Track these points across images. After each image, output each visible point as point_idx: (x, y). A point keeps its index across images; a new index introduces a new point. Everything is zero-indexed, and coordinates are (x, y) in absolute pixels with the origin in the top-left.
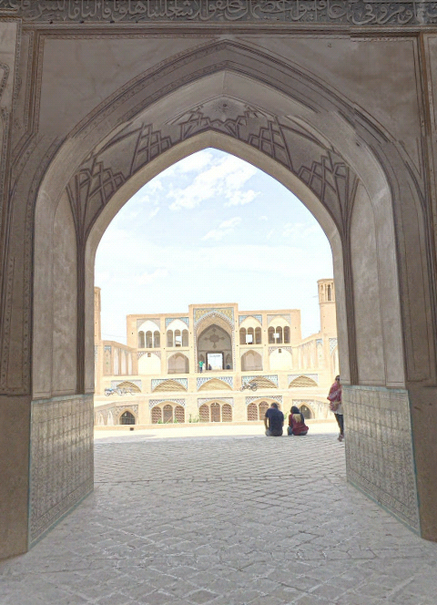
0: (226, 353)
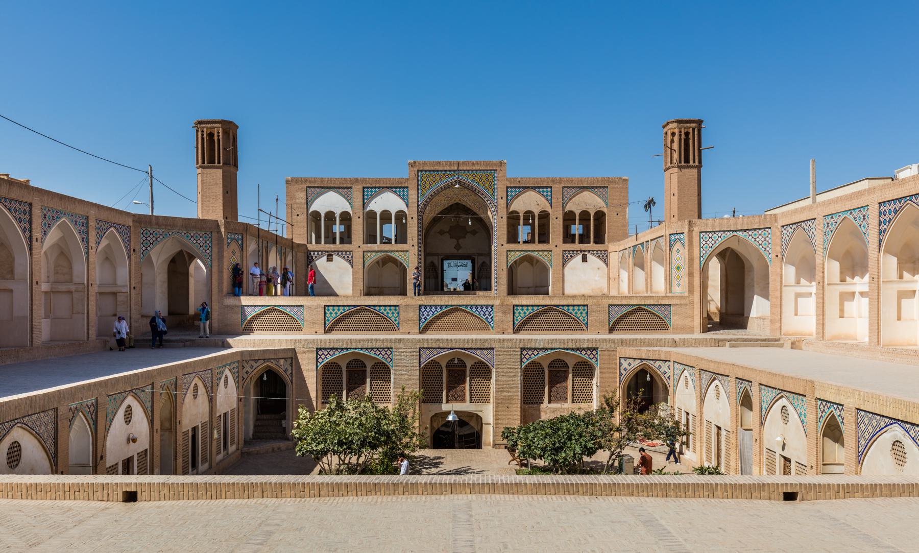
0: (479, 260)
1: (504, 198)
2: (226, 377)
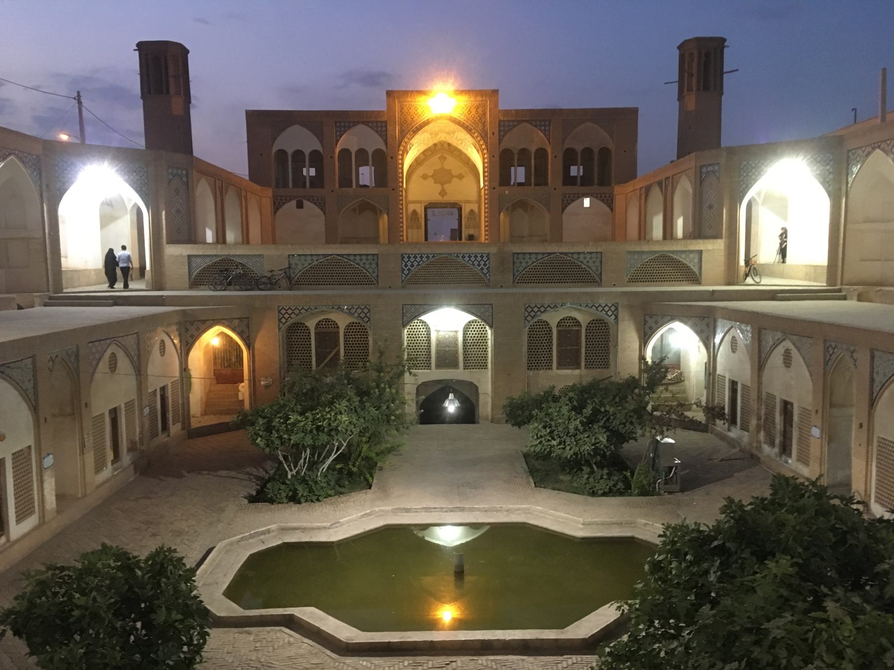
2: (163, 342)
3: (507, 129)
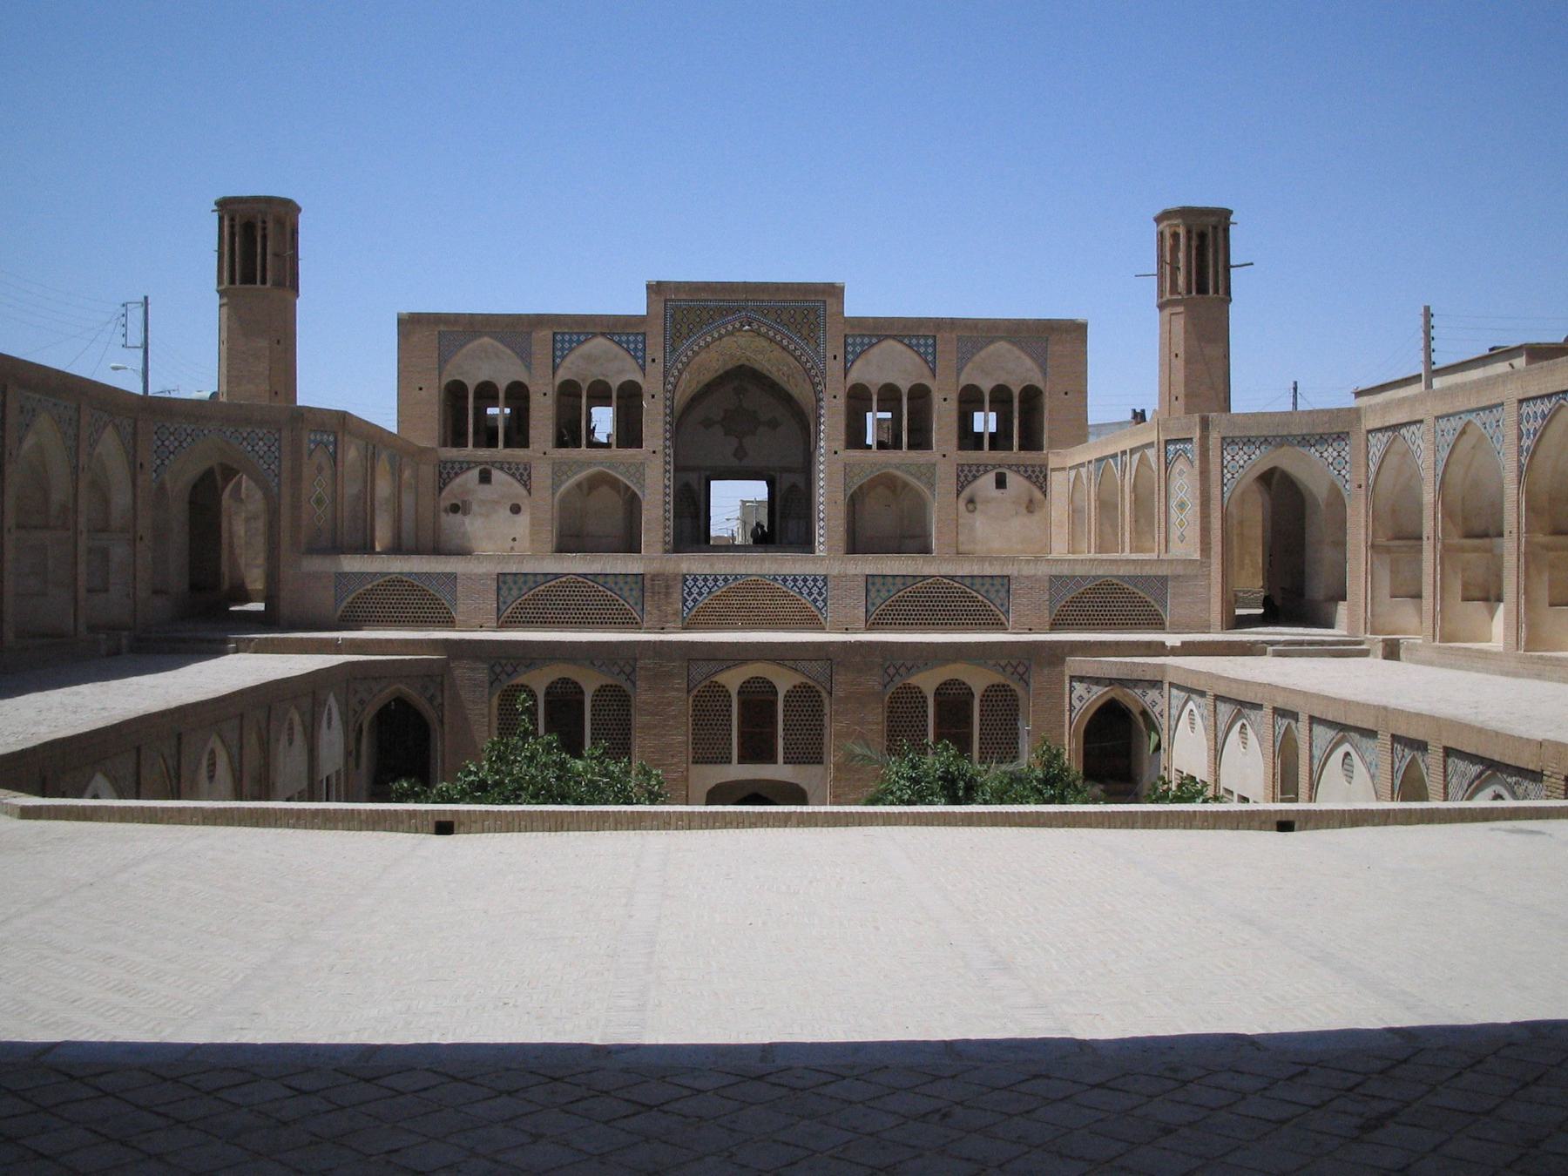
0: (785, 481)
1: (840, 358)
3: (858, 349)
